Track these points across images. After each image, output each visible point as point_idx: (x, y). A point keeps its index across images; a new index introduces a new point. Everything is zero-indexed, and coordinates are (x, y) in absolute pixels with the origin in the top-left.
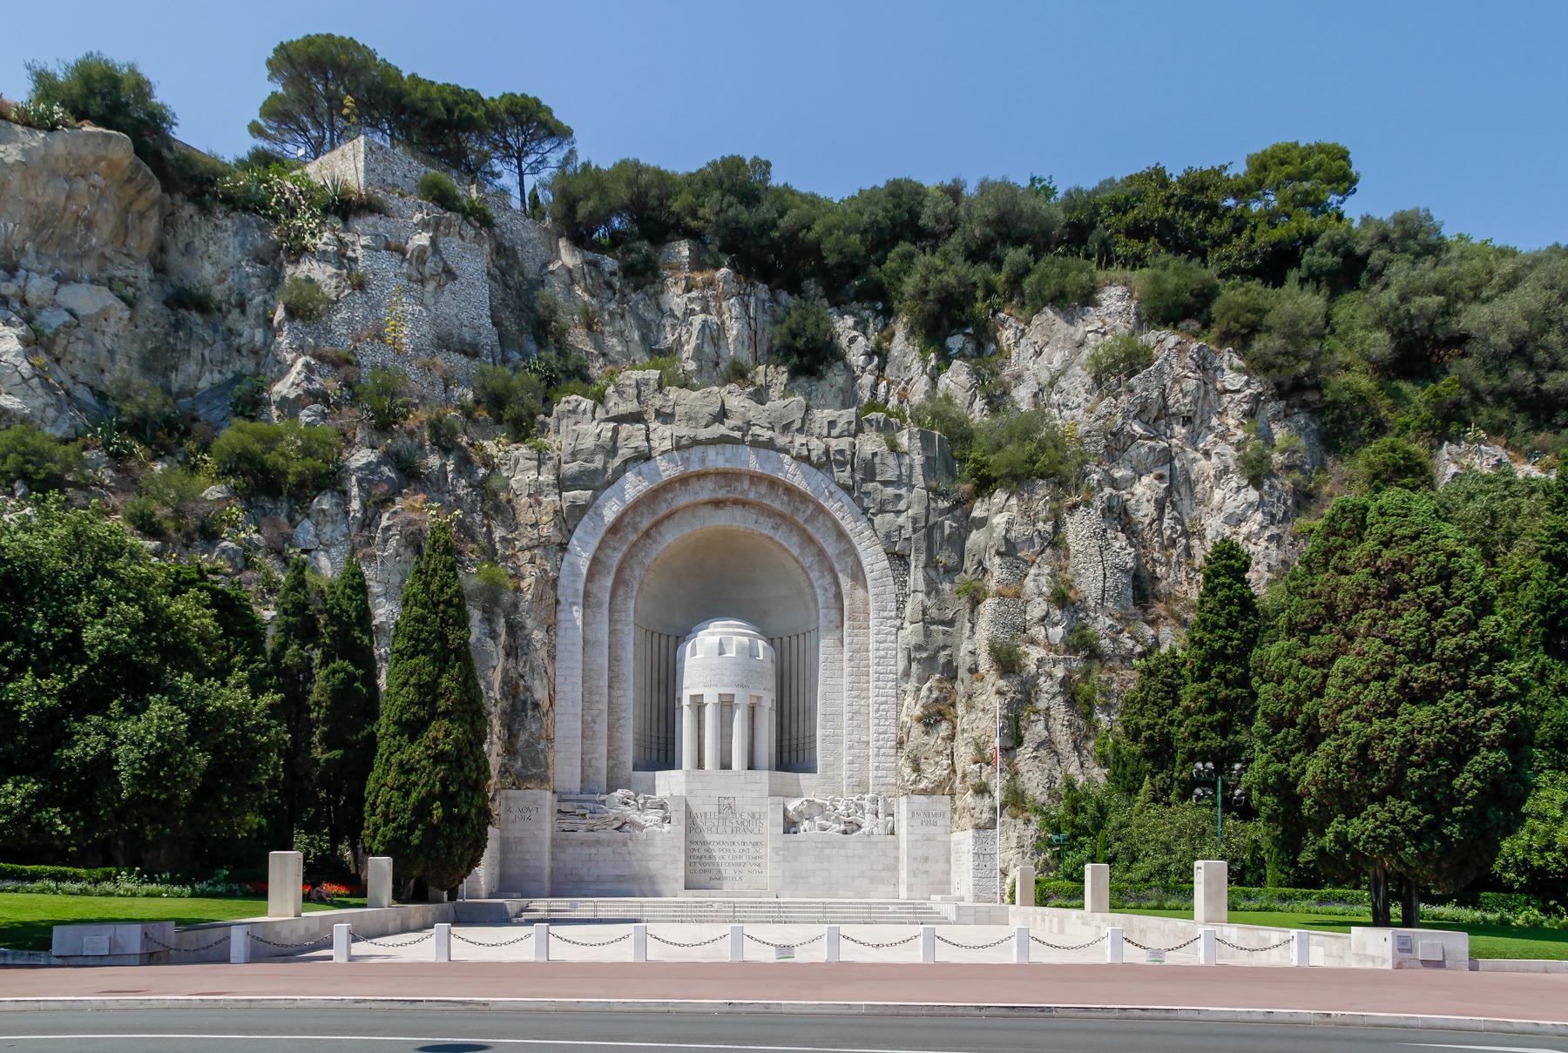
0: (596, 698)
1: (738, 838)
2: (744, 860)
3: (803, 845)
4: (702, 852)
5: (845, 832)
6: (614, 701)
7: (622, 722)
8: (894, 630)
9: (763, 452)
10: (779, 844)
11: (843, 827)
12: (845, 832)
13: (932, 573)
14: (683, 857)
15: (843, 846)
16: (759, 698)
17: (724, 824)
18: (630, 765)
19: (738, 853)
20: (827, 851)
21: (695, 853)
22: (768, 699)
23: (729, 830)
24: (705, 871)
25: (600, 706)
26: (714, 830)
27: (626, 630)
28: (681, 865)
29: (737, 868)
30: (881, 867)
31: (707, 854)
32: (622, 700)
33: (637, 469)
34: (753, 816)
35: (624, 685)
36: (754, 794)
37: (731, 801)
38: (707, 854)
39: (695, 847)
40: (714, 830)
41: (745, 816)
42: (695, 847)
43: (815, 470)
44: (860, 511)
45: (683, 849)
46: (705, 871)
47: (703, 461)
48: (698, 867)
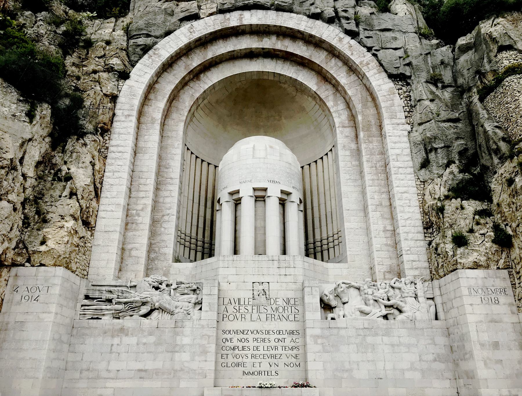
0: (142, 194)
1: (274, 325)
2: (280, 351)
3: (343, 332)
4: (235, 343)
5: (386, 317)
6: (161, 200)
7: (166, 218)
8: (406, 133)
9: (286, 14)
10: (318, 332)
11: (384, 312)
12: (386, 317)
13: (433, 88)
14: (212, 348)
15: (387, 333)
16: (288, 194)
17: (258, 311)
18: (170, 257)
19: (273, 344)
20: (369, 339)
21: (228, 344)
22: (296, 196)
23: (263, 317)
24: (238, 365)
25: (143, 201)
26: (248, 316)
27: (176, 145)
28: (211, 357)
29: (273, 361)
30: (431, 357)
31: (240, 345)
32: (168, 200)
33: (189, 25)
34: (288, 301)
35: (170, 187)
36: (289, 279)
37: (265, 286)
38: (240, 345)
39: (229, 336)
40: (248, 316)
41: (280, 302)
42: (229, 336)
43: (326, 25)
44: (365, 50)
45: (213, 340)
46: (238, 365)
47: (241, 19)
48: (231, 360)
